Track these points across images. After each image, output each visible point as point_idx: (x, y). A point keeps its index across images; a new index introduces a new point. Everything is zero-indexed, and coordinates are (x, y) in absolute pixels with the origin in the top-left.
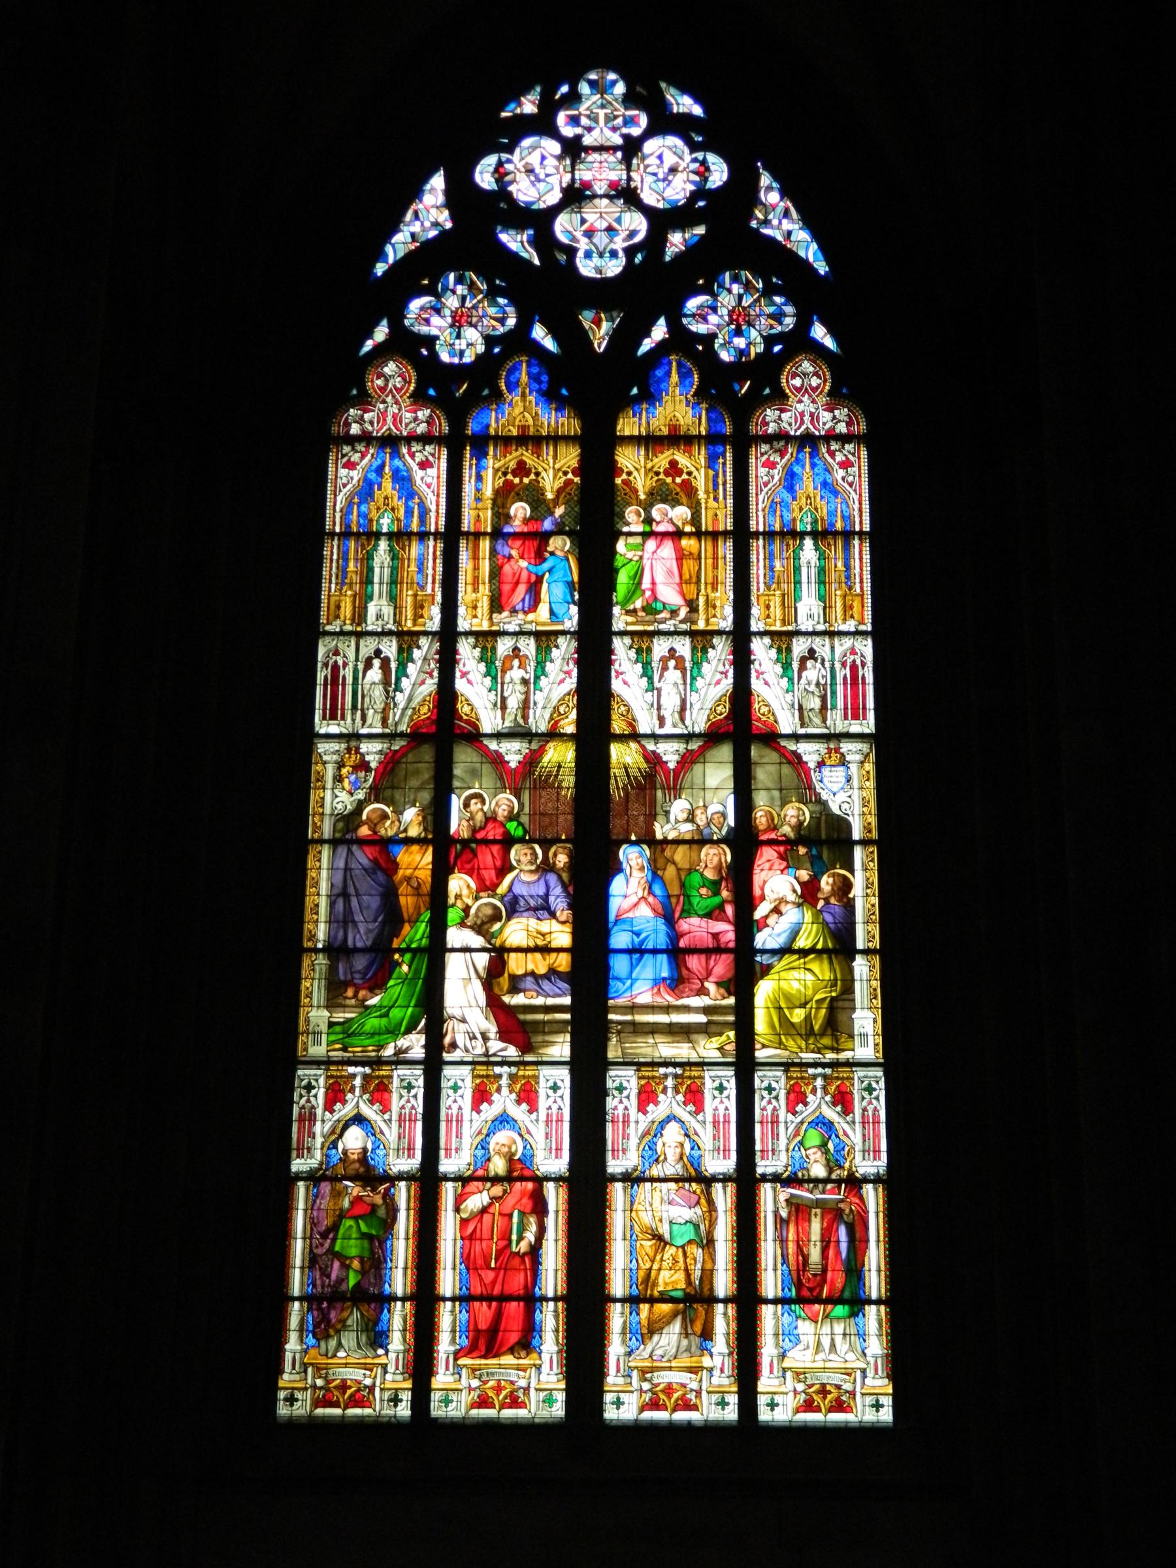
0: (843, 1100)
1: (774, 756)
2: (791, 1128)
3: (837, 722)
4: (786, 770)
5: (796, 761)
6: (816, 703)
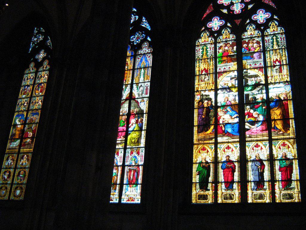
0: (138, 153)
1: (134, 102)
2: (131, 158)
3: (144, 95)
4: (136, 103)
5: (137, 102)
6: (141, 93)
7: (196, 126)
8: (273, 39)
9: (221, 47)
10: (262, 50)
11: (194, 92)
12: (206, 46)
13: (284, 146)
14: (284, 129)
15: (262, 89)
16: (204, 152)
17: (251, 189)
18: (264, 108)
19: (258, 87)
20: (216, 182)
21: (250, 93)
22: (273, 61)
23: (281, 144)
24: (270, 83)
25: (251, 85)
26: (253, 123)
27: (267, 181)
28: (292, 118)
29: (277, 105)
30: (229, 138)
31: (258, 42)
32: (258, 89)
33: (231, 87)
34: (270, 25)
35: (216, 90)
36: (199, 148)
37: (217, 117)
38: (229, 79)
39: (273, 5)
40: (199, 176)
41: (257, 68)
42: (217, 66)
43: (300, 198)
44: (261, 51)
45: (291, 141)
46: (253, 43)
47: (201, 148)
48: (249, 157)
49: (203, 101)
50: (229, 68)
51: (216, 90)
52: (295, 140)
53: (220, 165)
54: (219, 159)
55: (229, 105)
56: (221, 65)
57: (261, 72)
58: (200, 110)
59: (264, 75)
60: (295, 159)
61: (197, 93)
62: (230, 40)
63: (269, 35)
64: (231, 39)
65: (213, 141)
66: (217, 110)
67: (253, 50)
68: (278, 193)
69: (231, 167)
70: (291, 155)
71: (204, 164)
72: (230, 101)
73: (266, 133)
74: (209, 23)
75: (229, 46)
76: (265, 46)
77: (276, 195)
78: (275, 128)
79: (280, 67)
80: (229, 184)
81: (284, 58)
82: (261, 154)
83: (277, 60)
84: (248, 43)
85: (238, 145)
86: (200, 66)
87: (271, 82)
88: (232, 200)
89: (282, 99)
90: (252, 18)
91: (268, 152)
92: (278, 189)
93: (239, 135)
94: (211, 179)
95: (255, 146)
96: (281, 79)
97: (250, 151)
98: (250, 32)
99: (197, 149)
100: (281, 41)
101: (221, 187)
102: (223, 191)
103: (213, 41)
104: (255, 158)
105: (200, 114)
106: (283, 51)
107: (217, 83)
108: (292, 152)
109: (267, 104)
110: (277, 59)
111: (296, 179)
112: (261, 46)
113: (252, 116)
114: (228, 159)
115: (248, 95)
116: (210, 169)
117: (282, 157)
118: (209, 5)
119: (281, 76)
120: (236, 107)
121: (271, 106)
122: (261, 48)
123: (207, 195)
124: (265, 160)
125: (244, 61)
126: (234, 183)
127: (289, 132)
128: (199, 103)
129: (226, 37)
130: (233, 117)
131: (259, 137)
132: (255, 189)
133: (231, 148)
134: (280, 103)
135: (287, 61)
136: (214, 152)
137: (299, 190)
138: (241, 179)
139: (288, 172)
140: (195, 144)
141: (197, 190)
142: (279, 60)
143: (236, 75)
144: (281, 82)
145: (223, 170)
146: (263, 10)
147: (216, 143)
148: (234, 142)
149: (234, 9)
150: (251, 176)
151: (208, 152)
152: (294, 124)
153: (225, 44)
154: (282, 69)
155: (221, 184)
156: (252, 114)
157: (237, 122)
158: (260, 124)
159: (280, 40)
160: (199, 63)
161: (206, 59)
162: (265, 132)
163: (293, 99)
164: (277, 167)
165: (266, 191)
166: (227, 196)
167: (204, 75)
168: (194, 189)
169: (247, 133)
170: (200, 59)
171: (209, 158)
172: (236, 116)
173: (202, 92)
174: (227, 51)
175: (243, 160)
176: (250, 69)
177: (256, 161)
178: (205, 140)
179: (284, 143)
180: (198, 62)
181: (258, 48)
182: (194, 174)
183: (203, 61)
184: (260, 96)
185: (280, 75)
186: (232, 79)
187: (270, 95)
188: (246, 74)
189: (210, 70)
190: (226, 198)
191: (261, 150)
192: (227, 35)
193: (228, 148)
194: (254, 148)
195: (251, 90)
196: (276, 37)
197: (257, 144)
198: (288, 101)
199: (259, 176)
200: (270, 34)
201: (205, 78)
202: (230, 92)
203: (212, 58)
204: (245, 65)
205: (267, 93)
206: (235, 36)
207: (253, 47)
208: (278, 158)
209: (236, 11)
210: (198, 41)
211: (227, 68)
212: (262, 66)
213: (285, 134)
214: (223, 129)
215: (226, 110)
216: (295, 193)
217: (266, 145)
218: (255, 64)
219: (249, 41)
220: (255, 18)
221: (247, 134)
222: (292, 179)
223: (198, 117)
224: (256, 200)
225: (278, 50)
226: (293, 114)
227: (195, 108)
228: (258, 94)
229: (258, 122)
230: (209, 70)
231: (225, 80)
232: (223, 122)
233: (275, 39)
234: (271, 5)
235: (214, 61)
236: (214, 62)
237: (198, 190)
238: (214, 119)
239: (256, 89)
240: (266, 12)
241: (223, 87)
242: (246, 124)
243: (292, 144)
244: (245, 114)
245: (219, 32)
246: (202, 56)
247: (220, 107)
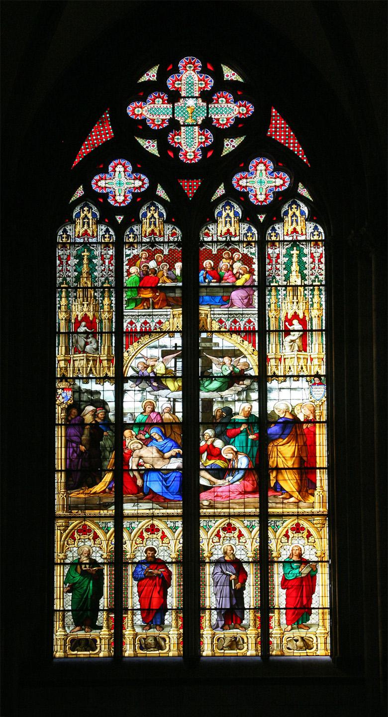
7: (61, 471)
8: (291, 256)
9: (136, 258)
10: (256, 284)
11: (54, 379)
12: (89, 251)
13: (298, 532)
14: (299, 491)
15: (248, 389)
16: (87, 537)
17: (211, 626)
18: (251, 437)
19: (238, 384)
20: (119, 609)
21: (215, 395)
22: (286, 317)
23: (289, 526)
24: (272, 376)
25: (220, 377)
26: (220, 473)
27: (249, 609)
28: (323, 468)
29: (284, 433)
30: (156, 506)
31: (246, 260)
32: (239, 388)
33: (162, 377)
34: (286, 213)
35: (119, 380)
36: (69, 528)
37: (122, 450)
38: (157, 353)
39: (298, 151)
40: (71, 594)
41: (238, 332)
42: (123, 312)
43: (329, 647)
44: (255, 286)
45: (315, 522)
46: (232, 258)
47: (76, 526)
48: (206, 554)
49: (82, 407)
50: (160, 323)
51: (119, 380)
52: (326, 520)
53: (130, 569)
54: (127, 557)
55: (157, 424)
56: (136, 312)
57: (250, 342)
58: (72, 431)
59: (256, 353)
60: (322, 561)
61: (63, 385)
62: (164, 242)
63: (279, 241)
64: (166, 240)
65: (111, 511)
66: (122, 434)
67: (231, 279)
68: (276, 636)
69: (158, 575)
70: (313, 552)
71: (85, 567)
72: (160, 411)
73: (254, 499)
74: (97, 177)
75: (160, 260)
76: (267, 273)
77: (271, 639)
78: (278, 489)
79: (301, 336)
80: (154, 615)
81: (315, 313)
82: (238, 547)
83: (295, 316)
84: (217, 258)
85: (179, 524)
86: (71, 309)
87: (274, 373)
88: (160, 651)
89: (302, 420)
90: (234, 182)
91: (256, 545)
92: (277, 628)
93: (183, 501)
94: (104, 602)
95: (224, 529)
96: (302, 368)
97: (211, 540)
98: (226, 224)
99: (65, 530)
100: (312, 263)
101: (132, 620)
102: (138, 630)
103: (111, 235)
104: (223, 555)
105: (72, 441)
106: (316, 292)
107: (123, 361)
108: (316, 546)
109: (259, 429)
110: (295, 313)
111: (320, 607)
112: (256, 273)
113: (219, 456)
114: (151, 557)
115: (209, 403)
116: (104, 579)
117: (292, 554)
118: (100, 117)
119: (302, 361)
120: (177, 430)
121: (271, 434)
122: (256, 277)
123: (95, 641)
124: (249, 562)
125: (204, 309)
126: (168, 613)
127: (311, 499)
128: (68, 410)
129: (153, 230)
130: (167, 455)
131: (234, 507)
132: (220, 626)
133: (161, 531)
134: (292, 426)
135: (324, 322)
136: (112, 538)
137: (328, 629)
138: (184, 605)
139: (303, 587)
140: (60, 517)
141: (66, 628)
142: (301, 316)
143: (180, 343)
144: (303, 376)
145: (137, 582)
146: (267, 161)
147: (119, 518)
148: (168, 516)
149: (180, 143)
150: (211, 597)
151: (96, 537)
152: (325, 483)
153: (148, 251)
154: (309, 342)
155: (133, 614)
156: (220, 450)
157: (178, 469)
158: (239, 476)
159: (311, 260)
160: (67, 297)
161: (91, 288)
162: (250, 496)
163: (329, 422)
164: (277, 579)
165: (248, 632)
166: (149, 641)
167: (85, 336)
168: (58, 625)
169: (203, 495)
170: (69, 287)
171: (100, 550)
172: (174, 454)
173: (77, 382)
174: (155, 272)
175: (191, 559)
176: (219, 332)
177: (226, 562)
178: (87, 508)
179: (298, 524)
180: (64, 294)
181: (247, 276)
182: (57, 592)
183: (80, 293)
184: (244, 407)
185: (302, 357)
186: (165, 354)
187: (270, 407)
188: (208, 345)
189: (101, 321)
190: (144, 646)
191: (239, 539)
192: (155, 224)
193: (153, 529)
194: (221, 533)
195: (219, 390)
196: (301, 250)
197: (229, 524)
198: (315, 426)
199: (231, 597)
200: (284, 241)
201: (86, 344)
202: (158, 389)
203: (109, 288)
204: (206, 320)
205: (263, 401)
206: (178, 231)
207: (230, 273)
208: (280, 559)
209: (187, 152)
210: (65, 231)
211: (153, 321)
212: (254, 327)
213: (301, 504)
214: (139, 482)
215: (147, 436)
216: (316, 637)
217: (252, 527)
218: (235, 322)
219: (220, 251)
220: (243, 183)
221: (205, 499)
222: (312, 606)
223: (66, 447)
224: (223, 651)
225: (302, 289)
226: (326, 459)
227: (58, 424)
228: (239, 400)
229: (233, 470)
230: (97, 321)
231: (144, 355)
232: (138, 465)
233: (295, 256)
234: (294, 151)
235: (113, 299)
236: (114, 302)
237: (69, 627)
238: (113, 455)
239: (233, 388)
240: (276, 169)
241: (141, 373)
242: (203, 473)
243: (317, 528)
244: (201, 449)
245: (132, 213)
246: (78, 279)
247: (130, 426)
